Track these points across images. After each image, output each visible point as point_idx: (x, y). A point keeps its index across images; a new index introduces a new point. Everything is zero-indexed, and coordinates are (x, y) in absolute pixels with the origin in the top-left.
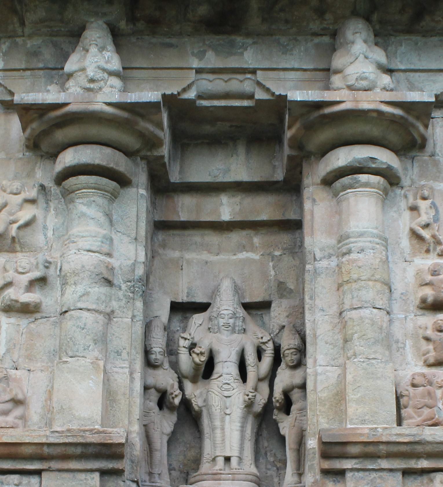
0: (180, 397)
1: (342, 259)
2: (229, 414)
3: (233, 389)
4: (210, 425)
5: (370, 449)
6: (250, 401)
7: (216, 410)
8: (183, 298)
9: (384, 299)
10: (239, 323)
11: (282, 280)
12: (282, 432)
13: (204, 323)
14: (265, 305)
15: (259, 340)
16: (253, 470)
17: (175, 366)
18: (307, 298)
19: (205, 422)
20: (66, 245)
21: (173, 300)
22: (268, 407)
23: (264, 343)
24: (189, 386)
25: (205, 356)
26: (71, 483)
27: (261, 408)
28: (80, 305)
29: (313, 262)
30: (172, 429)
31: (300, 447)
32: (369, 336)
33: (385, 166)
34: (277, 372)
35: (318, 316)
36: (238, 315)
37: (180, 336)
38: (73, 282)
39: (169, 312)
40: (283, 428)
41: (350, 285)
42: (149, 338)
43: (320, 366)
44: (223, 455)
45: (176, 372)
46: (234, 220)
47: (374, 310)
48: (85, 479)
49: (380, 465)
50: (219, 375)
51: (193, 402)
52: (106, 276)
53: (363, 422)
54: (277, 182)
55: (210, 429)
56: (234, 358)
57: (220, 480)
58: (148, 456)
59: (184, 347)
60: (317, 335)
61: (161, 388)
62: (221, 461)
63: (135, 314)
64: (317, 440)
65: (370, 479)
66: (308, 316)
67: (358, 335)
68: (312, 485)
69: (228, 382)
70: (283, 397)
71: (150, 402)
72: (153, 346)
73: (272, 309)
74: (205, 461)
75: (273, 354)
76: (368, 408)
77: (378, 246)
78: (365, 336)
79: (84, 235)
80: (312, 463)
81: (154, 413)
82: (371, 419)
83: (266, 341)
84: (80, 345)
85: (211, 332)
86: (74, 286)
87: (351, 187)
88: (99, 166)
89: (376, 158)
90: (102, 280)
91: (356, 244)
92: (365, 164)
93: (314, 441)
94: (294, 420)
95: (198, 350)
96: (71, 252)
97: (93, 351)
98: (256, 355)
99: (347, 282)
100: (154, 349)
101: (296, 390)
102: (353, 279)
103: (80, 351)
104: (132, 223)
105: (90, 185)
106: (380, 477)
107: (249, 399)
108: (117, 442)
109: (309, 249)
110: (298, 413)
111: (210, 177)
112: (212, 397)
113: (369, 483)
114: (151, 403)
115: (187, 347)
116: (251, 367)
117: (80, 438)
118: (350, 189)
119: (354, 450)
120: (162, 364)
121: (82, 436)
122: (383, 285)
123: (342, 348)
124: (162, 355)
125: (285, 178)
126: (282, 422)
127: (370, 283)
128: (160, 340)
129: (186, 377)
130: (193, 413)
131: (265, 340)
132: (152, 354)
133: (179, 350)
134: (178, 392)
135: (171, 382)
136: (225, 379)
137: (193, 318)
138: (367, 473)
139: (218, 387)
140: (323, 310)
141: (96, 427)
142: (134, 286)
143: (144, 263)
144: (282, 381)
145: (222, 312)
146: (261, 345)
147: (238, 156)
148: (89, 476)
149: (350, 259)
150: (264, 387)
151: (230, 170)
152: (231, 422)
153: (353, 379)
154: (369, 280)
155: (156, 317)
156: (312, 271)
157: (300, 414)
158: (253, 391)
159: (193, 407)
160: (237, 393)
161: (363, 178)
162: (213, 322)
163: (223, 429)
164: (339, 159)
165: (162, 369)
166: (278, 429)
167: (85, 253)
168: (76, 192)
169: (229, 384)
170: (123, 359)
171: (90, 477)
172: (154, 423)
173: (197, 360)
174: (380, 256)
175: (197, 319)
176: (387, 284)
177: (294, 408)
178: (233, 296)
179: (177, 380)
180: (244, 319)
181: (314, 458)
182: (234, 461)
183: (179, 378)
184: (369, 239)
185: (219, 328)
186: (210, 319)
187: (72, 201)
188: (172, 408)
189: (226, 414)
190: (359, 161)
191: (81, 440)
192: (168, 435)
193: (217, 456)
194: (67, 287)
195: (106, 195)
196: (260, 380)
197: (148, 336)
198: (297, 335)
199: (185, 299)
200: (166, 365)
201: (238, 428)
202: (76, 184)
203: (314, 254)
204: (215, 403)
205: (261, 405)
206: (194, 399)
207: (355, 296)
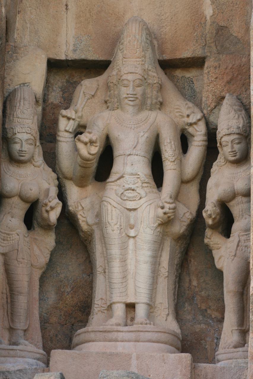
0: (59, 210)
2: (134, 237)
3: (141, 198)
4: (105, 252)
6: (166, 216)
7: (113, 231)
10: (152, 93)
11: (222, 24)
12: (218, 265)
13: (99, 93)
15: (183, 119)
21: (51, 56)
23: (191, 125)
27: (185, 227)
31: (243, 289)
34: (212, 170)
36: (150, 81)
37: (61, 114)
40: (220, 258)
42: (12, 118)
44: (124, 301)
45: (54, 171)
50: (118, 176)
51: (79, 217)
57: (116, 340)
61: (28, 195)
62: (119, 310)
69: (133, 187)
71: (12, 217)
72: (18, 129)
73: (205, 70)
75: (205, 141)
81: (18, 235)
83: (194, 120)
94: (236, 247)
95: (87, 137)
107: (165, 213)
110: (243, 235)
114: (13, 220)
115: (71, 130)
116: (169, 163)
124: (31, 144)
128: (27, 121)
129: (71, 179)
131: (192, 119)
132: (16, 143)
135: (46, 186)
136: (129, 181)
137: (81, 85)
139: (117, 195)
144: (217, 185)
145: (124, 77)
146: (187, 127)
157: (245, 237)
158: (171, 201)
159: (80, 225)
160: (146, 204)
162: (112, 92)
163: (124, 261)
165: (32, 167)
169: (133, 190)
172: (18, 251)
173: (84, 151)
177: (236, 227)
178: (143, 51)
182: (141, 311)
183: (58, 179)
185: (119, 101)
186: (108, 88)
188: (47, 227)
192: (41, 268)
193: (114, 303)
196: (183, 182)
197: (10, 114)
198: (243, 112)
200: (39, 159)
201: (148, 259)
204: (112, 219)
205: (185, 222)
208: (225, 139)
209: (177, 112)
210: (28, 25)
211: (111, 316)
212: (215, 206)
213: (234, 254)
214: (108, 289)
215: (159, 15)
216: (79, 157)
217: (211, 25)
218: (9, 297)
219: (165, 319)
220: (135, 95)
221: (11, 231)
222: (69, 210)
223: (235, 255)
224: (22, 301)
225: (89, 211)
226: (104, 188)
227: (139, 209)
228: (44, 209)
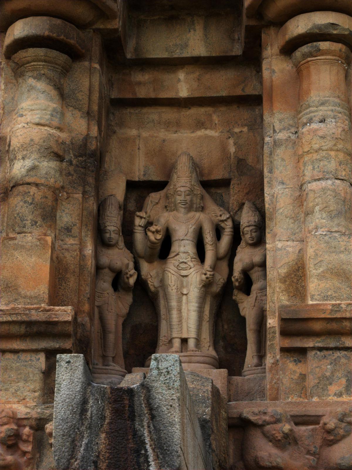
0: (135, 277)
1: (303, 129)
2: (186, 295)
3: (191, 268)
5: (334, 326)
6: (208, 280)
8: (138, 175)
9: (347, 170)
10: (197, 201)
11: (241, 157)
12: (242, 314)
13: (161, 202)
14: (225, 183)
15: (217, 218)
16: (212, 352)
17: (130, 244)
18: (266, 171)
19: (162, 303)
20: (14, 119)
21: (129, 179)
22: (228, 287)
23: (223, 221)
24: (145, 266)
25: (160, 234)
26: (15, 364)
27: (220, 288)
28: (27, 180)
29: (272, 134)
30: (127, 311)
32: (332, 208)
33: (346, 33)
34: (237, 251)
35: (278, 189)
36: (195, 192)
37: (136, 215)
38: (20, 157)
39: (124, 192)
40: (244, 309)
41: (310, 155)
42: (103, 217)
43: (280, 240)
44: (180, 337)
45: (132, 253)
46: (192, 96)
47: (336, 181)
48: (31, 360)
49: (344, 342)
50: (175, 254)
51: (149, 282)
52: (56, 150)
53: (326, 298)
54: (235, 57)
55: (166, 310)
56: (191, 235)
58: (101, 338)
59: (140, 226)
60: (277, 208)
62: (177, 343)
63: (86, 190)
64: (277, 319)
65: (334, 358)
66: (267, 190)
67: (320, 207)
68: (271, 366)
69: (185, 261)
70: (242, 276)
71: (104, 282)
72: (108, 224)
73: (231, 187)
74: (161, 344)
76: (330, 284)
77: (340, 115)
78: (327, 208)
79: (33, 108)
80: (272, 342)
81: (108, 294)
82: (334, 295)
83: (225, 218)
84: (28, 220)
85: (167, 210)
86: (22, 161)
87: (311, 55)
88: (49, 38)
89: (337, 23)
90: (52, 154)
91: (318, 113)
92: (326, 31)
93: (273, 320)
94: (254, 301)
96: (20, 126)
97: (40, 227)
98: (214, 232)
99: (308, 152)
100: (109, 228)
101: (256, 268)
102: (313, 149)
103: (27, 227)
104: (83, 97)
105: (40, 57)
106: (345, 356)
107: (207, 278)
108: (63, 320)
109: (268, 120)
110: (259, 293)
111: (167, 53)
112: (168, 276)
113: (332, 363)
114: (105, 284)
115: (142, 225)
116: (209, 246)
117: (24, 317)
118: (310, 57)
119: (317, 326)
120: (117, 243)
121: (27, 314)
122: (346, 155)
123: (303, 223)
124: (116, 234)
125: (244, 52)
126: (242, 303)
127: (333, 153)
128: (114, 219)
129: (143, 258)
130: (150, 294)
131: (224, 217)
132: (107, 233)
133: (134, 229)
134: (133, 271)
135: (126, 261)
136: (182, 257)
137: (149, 196)
138: (331, 352)
139: (174, 266)
140: (283, 183)
141: (43, 305)
142: (85, 161)
143: (96, 138)
144: (241, 260)
145: (178, 189)
146: (220, 223)
147: (195, 30)
148: (34, 356)
149: (310, 129)
150: (224, 266)
151: (187, 46)
152: (187, 302)
153: (314, 254)
154: (331, 150)
155: (111, 195)
156: (271, 143)
158: (211, 270)
159: (149, 288)
160: (194, 272)
161: (324, 45)
162: (170, 200)
163: (180, 310)
164: (298, 26)
165: (117, 249)
166: (238, 310)
167: (35, 127)
168: (25, 66)
169: (185, 263)
170: (73, 236)
171: (36, 357)
172: (108, 304)
173: (152, 237)
174: (343, 125)
175: (154, 197)
176: (350, 155)
177: (255, 287)
178: (190, 173)
179: (133, 260)
180: (202, 198)
181: (274, 337)
182: (191, 343)
183: (134, 258)
184: (330, 108)
185: (175, 206)
186: (167, 197)
187: (22, 75)
188: (127, 289)
189: (183, 294)
190: (319, 27)
191: (25, 318)
192: (123, 317)
193: (174, 338)
194: (16, 162)
195: (57, 68)
196: (218, 259)
197: (103, 214)
198: (258, 212)
199: (142, 178)
200: (121, 244)
201: (195, 309)
202: (26, 57)
203: (274, 126)
204: (171, 282)
206: (150, 279)
207: (316, 167)
208: (246, 229)
209: (213, 213)
210: (114, 159)
211: (171, 347)
212: (240, 274)
213: (253, 305)
214: (169, 330)
215: (200, 152)
216: (149, 242)
217: (234, 158)
218: (102, 335)
219: (207, 349)
220: (186, 201)
221: (104, 291)
222: (142, 278)
223: (254, 306)
224: (111, 337)
225: (155, 278)
226: (166, 263)
227: (189, 276)
228: (125, 276)
